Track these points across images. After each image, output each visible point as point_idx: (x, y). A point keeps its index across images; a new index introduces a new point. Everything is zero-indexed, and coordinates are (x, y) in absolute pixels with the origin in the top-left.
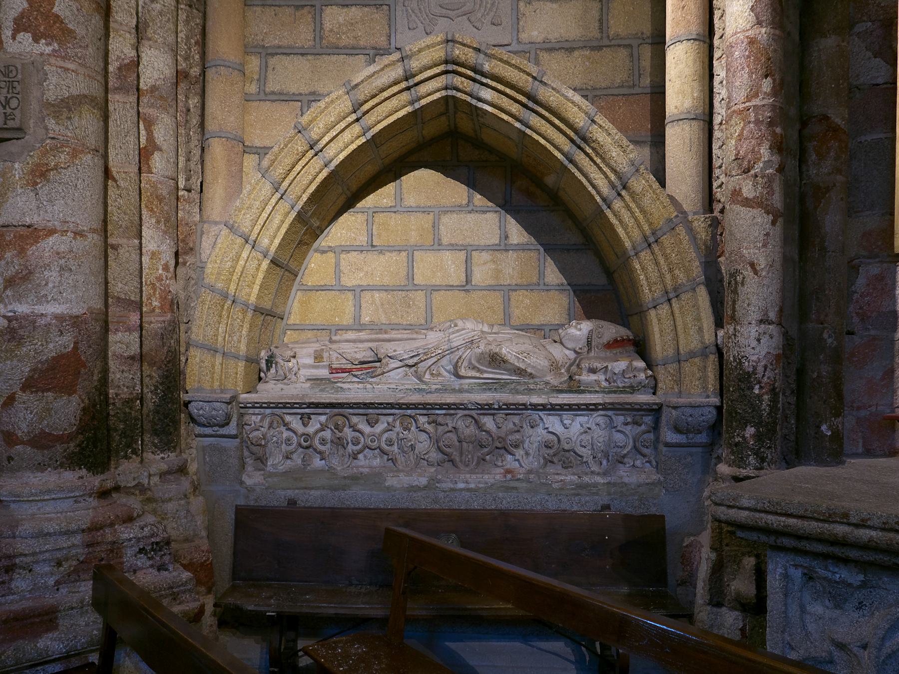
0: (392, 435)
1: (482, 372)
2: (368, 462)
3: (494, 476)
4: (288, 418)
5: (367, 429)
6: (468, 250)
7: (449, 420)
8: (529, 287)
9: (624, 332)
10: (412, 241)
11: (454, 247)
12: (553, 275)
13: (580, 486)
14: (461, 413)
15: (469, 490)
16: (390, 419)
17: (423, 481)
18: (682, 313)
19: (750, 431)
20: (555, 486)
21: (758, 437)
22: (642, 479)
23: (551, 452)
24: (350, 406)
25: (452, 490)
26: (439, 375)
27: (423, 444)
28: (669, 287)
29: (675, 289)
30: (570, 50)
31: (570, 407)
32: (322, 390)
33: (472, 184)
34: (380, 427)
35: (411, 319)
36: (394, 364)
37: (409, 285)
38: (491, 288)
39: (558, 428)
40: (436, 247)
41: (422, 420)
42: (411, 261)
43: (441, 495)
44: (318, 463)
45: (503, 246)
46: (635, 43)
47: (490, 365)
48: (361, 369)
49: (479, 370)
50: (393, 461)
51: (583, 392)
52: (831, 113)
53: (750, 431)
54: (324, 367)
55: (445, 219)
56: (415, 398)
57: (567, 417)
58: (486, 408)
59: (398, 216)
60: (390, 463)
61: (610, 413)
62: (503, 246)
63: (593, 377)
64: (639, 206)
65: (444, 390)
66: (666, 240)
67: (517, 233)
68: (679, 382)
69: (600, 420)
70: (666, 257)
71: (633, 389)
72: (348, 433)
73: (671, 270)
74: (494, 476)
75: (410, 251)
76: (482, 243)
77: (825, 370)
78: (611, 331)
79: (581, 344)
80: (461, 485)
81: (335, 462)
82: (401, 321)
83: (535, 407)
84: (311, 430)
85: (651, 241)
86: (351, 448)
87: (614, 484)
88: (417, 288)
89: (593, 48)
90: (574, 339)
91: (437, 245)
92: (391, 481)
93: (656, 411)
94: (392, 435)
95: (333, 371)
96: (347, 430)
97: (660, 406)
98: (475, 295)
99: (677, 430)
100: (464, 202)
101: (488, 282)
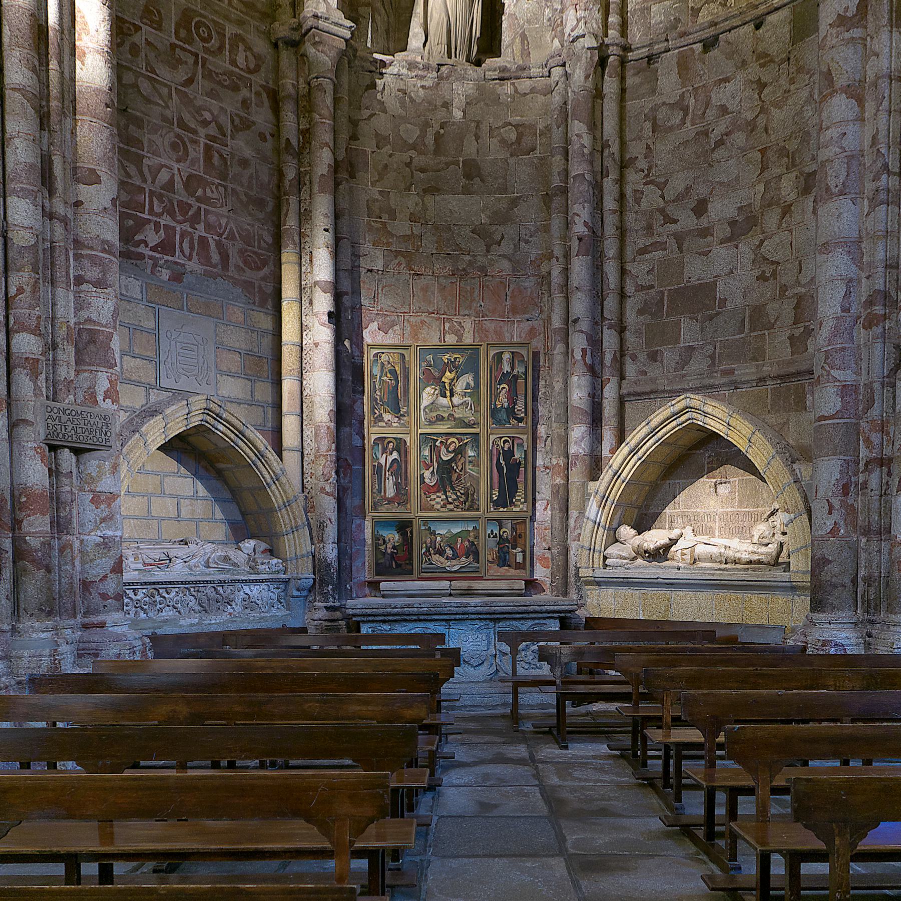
0: (178, 598)
1: (218, 564)
2: (168, 613)
3: (225, 617)
4: (127, 591)
5: (166, 596)
6: (178, 498)
7: (203, 589)
8: (207, 520)
9: (268, 547)
10: (150, 491)
11: (171, 496)
12: (219, 515)
13: (261, 618)
14: (210, 585)
15: (217, 623)
16: (177, 590)
17: (196, 621)
18: (299, 538)
19: (330, 587)
20: (251, 619)
21: (333, 590)
22: (284, 613)
23: (246, 603)
24: (158, 583)
25: (210, 624)
26: (198, 566)
27: (193, 603)
28: (293, 526)
29: (296, 527)
30: (240, 404)
31: (253, 581)
32: (144, 576)
33: (179, 461)
34: (173, 594)
35: (151, 536)
36: (178, 561)
37: (149, 516)
38: (190, 520)
39: (248, 591)
40: (162, 495)
41: (192, 589)
42: (149, 501)
43: (205, 627)
44: (143, 615)
45: (195, 497)
46: (265, 405)
47: (223, 561)
48: (161, 564)
49: (218, 564)
50: (179, 612)
51: (259, 574)
52: (348, 458)
53: (330, 587)
54: (140, 563)
55: (166, 479)
56: (192, 579)
57: (252, 585)
58: (222, 583)
59: (142, 476)
60: (177, 613)
61: (269, 583)
62: (195, 497)
63: (263, 567)
64: (282, 489)
65: (202, 574)
66: (294, 505)
67: (202, 491)
68: (297, 568)
69: (266, 587)
70: (293, 513)
71: (278, 572)
72: (158, 598)
73: (294, 519)
74: (225, 617)
75: (148, 495)
76: (185, 494)
77: (348, 562)
78: (263, 546)
79: (251, 551)
80: (213, 622)
81: (151, 614)
82: (145, 537)
83: (243, 581)
84: (138, 597)
85: (287, 504)
86: (159, 606)
87: (273, 616)
88: (153, 518)
89: (248, 405)
90: (248, 548)
91: (163, 494)
92: (182, 622)
93: (286, 582)
94: (178, 598)
95: (145, 564)
96: (157, 597)
97: (289, 579)
98: (182, 523)
99: (298, 590)
100: (176, 471)
101: (188, 517)
